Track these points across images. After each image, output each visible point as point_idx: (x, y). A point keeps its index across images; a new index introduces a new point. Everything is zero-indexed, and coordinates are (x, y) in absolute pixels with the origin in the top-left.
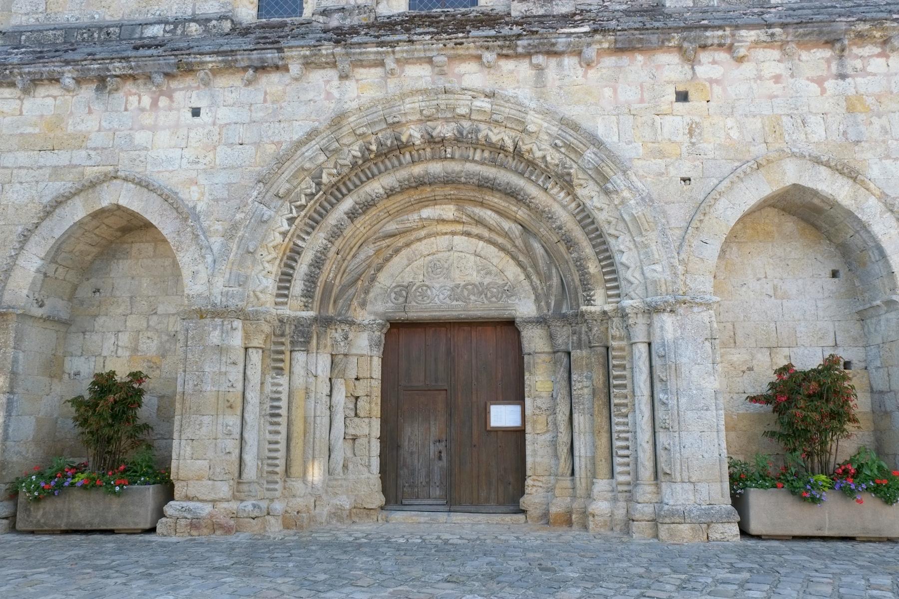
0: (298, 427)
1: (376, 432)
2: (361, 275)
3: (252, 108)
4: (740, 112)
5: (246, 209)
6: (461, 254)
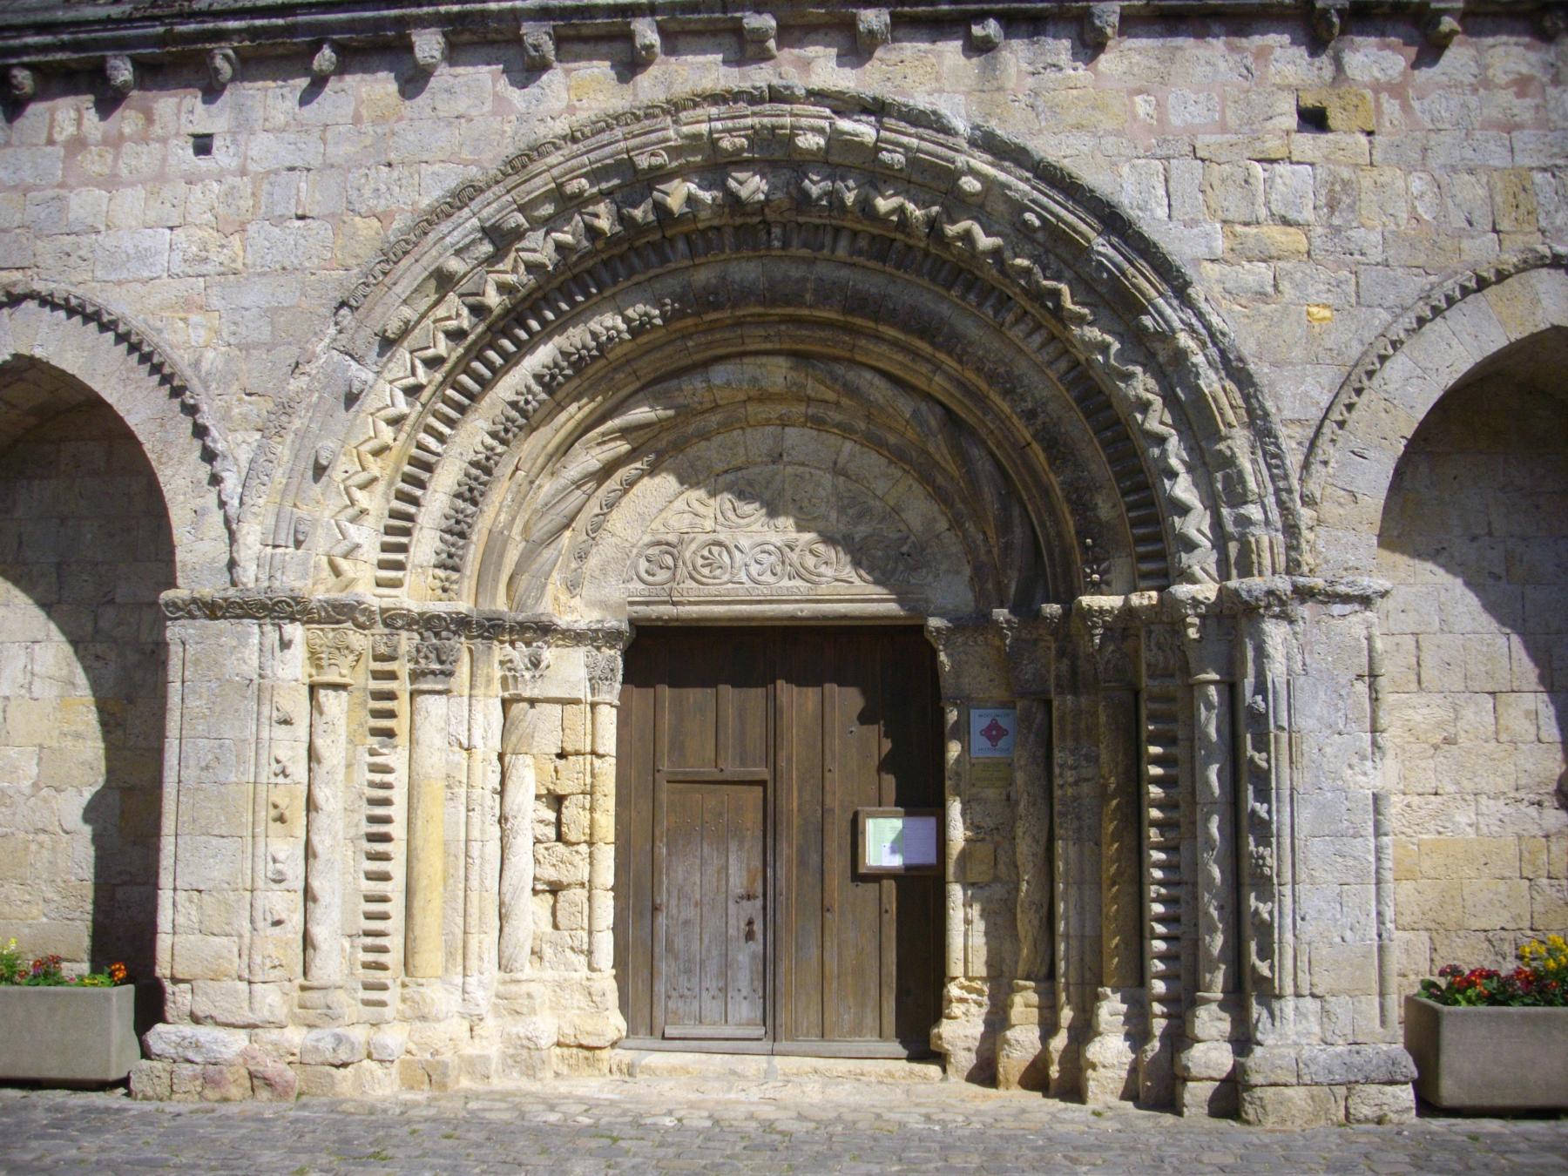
0: (432, 865)
1: (606, 874)
2: (572, 519)
3: (329, 135)
4: (1442, 160)
5: (311, 369)
6: (801, 469)
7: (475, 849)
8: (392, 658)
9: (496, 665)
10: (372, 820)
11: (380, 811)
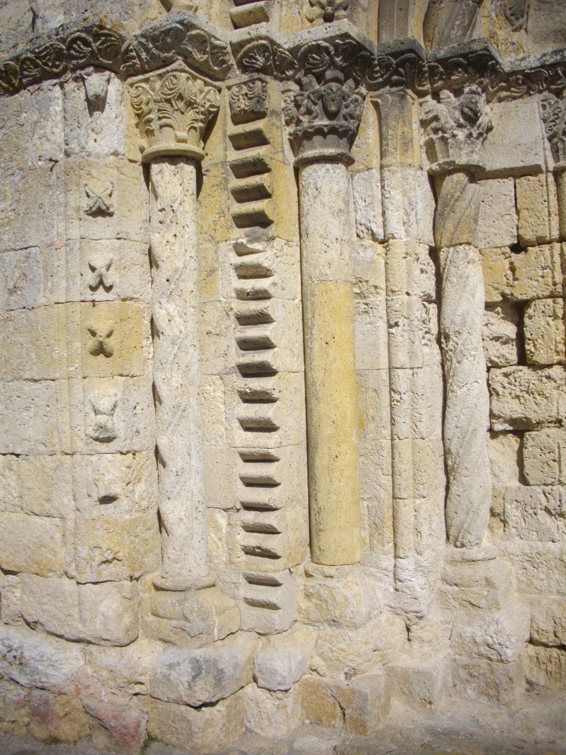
0: (338, 404)
7: (403, 380)
8: (260, 115)
9: (416, 126)
10: (247, 345)
11: (254, 332)
